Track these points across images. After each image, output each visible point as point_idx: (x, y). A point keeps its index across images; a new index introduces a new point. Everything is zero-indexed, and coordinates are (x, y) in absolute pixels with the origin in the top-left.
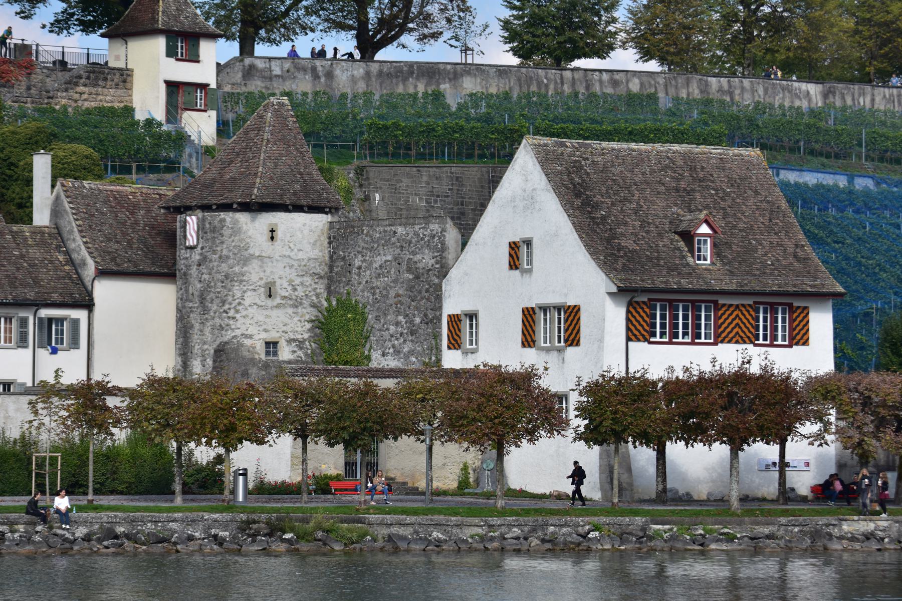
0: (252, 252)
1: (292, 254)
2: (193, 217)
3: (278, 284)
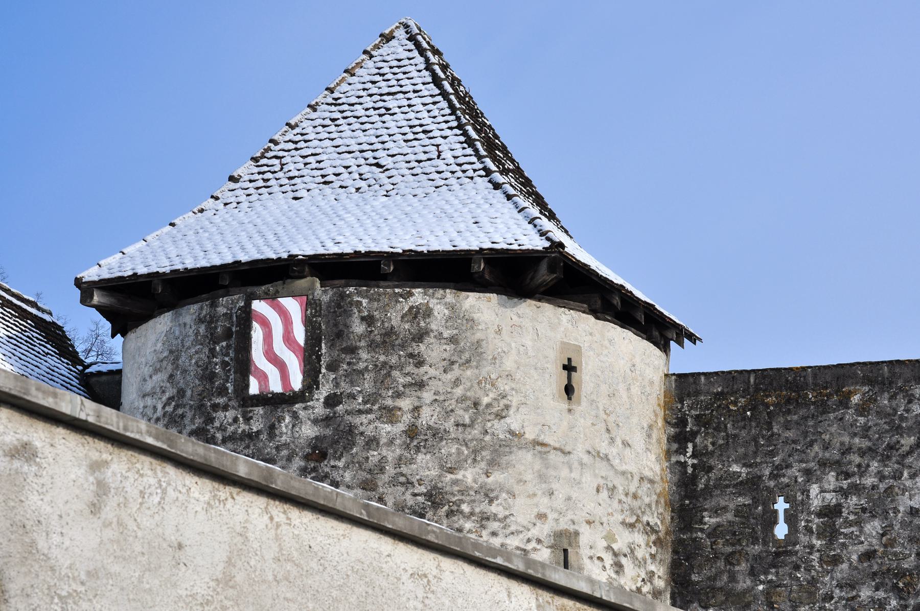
0: (515, 427)
1: (613, 452)
2: (292, 305)
3: (584, 540)
